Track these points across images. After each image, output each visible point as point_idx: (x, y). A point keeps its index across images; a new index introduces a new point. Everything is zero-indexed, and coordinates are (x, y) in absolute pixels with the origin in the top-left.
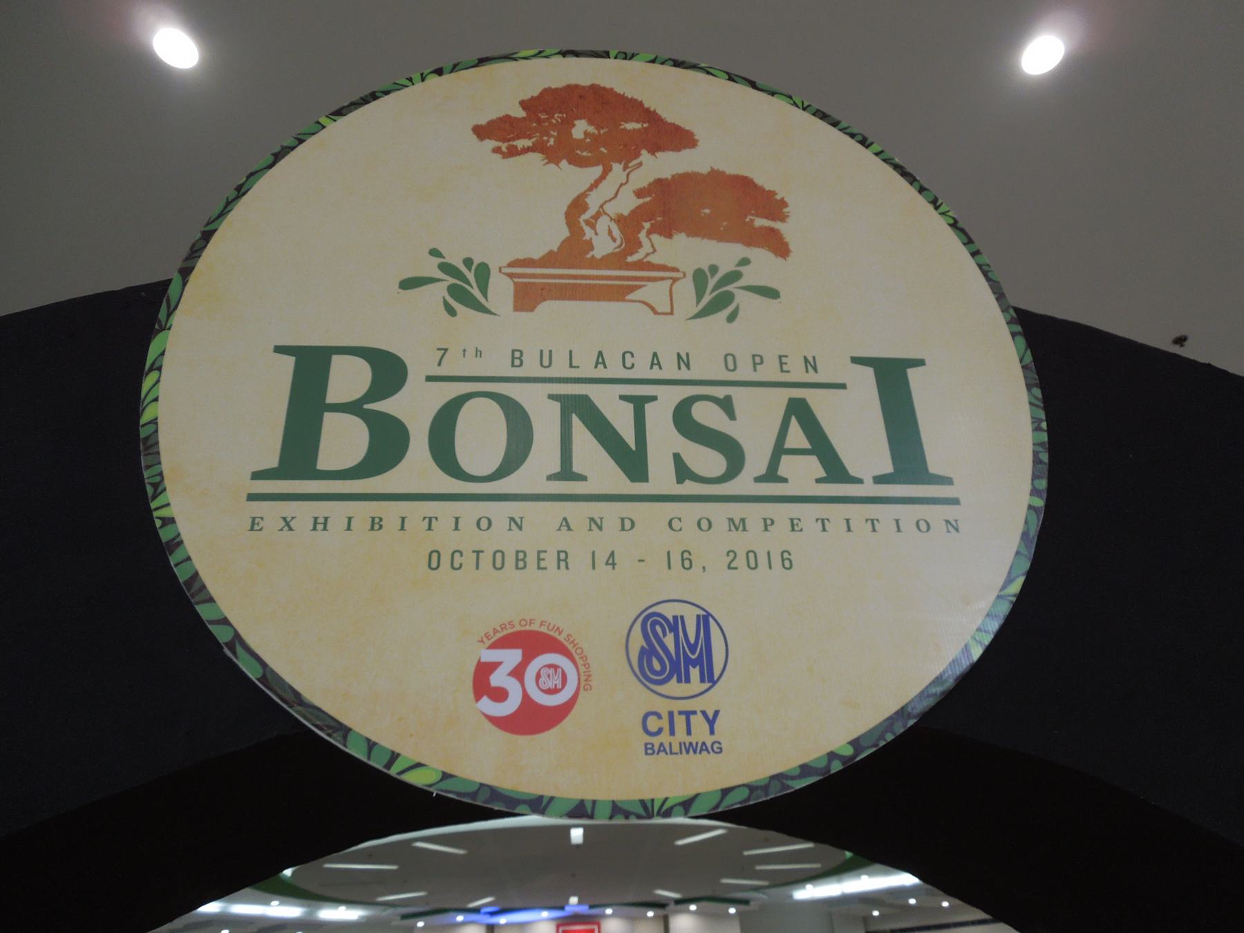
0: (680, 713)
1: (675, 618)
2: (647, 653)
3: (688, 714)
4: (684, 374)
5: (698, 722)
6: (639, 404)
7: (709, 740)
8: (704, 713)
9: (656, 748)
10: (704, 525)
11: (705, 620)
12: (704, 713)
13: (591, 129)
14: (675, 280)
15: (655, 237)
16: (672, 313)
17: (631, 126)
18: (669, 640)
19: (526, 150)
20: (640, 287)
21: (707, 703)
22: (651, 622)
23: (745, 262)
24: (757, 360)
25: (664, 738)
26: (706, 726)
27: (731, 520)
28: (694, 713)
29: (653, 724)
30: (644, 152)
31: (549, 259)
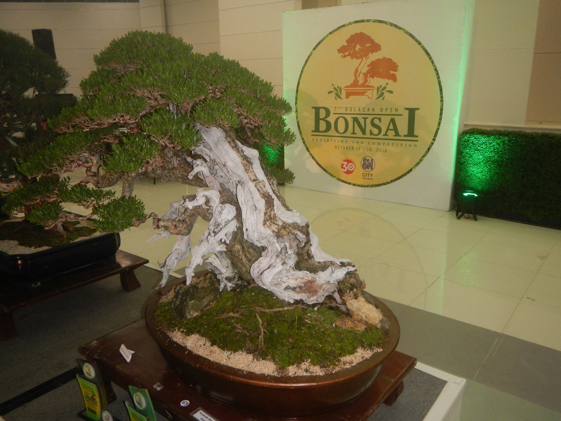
2: (364, 164)
3: (369, 174)
4: (373, 113)
5: (370, 175)
6: (365, 119)
7: (371, 178)
10: (374, 143)
11: (372, 160)
13: (360, 47)
14: (373, 90)
15: (370, 78)
16: (372, 98)
17: (368, 45)
18: (367, 163)
19: (348, 55)
20: (367, 92)
22: (364, 159)
23: (387, 84)
24: (386, 109)
25: (365, 177)
27: (378, 143)
29: (364, 175)
30: (370, 53)
31: (351, 86)
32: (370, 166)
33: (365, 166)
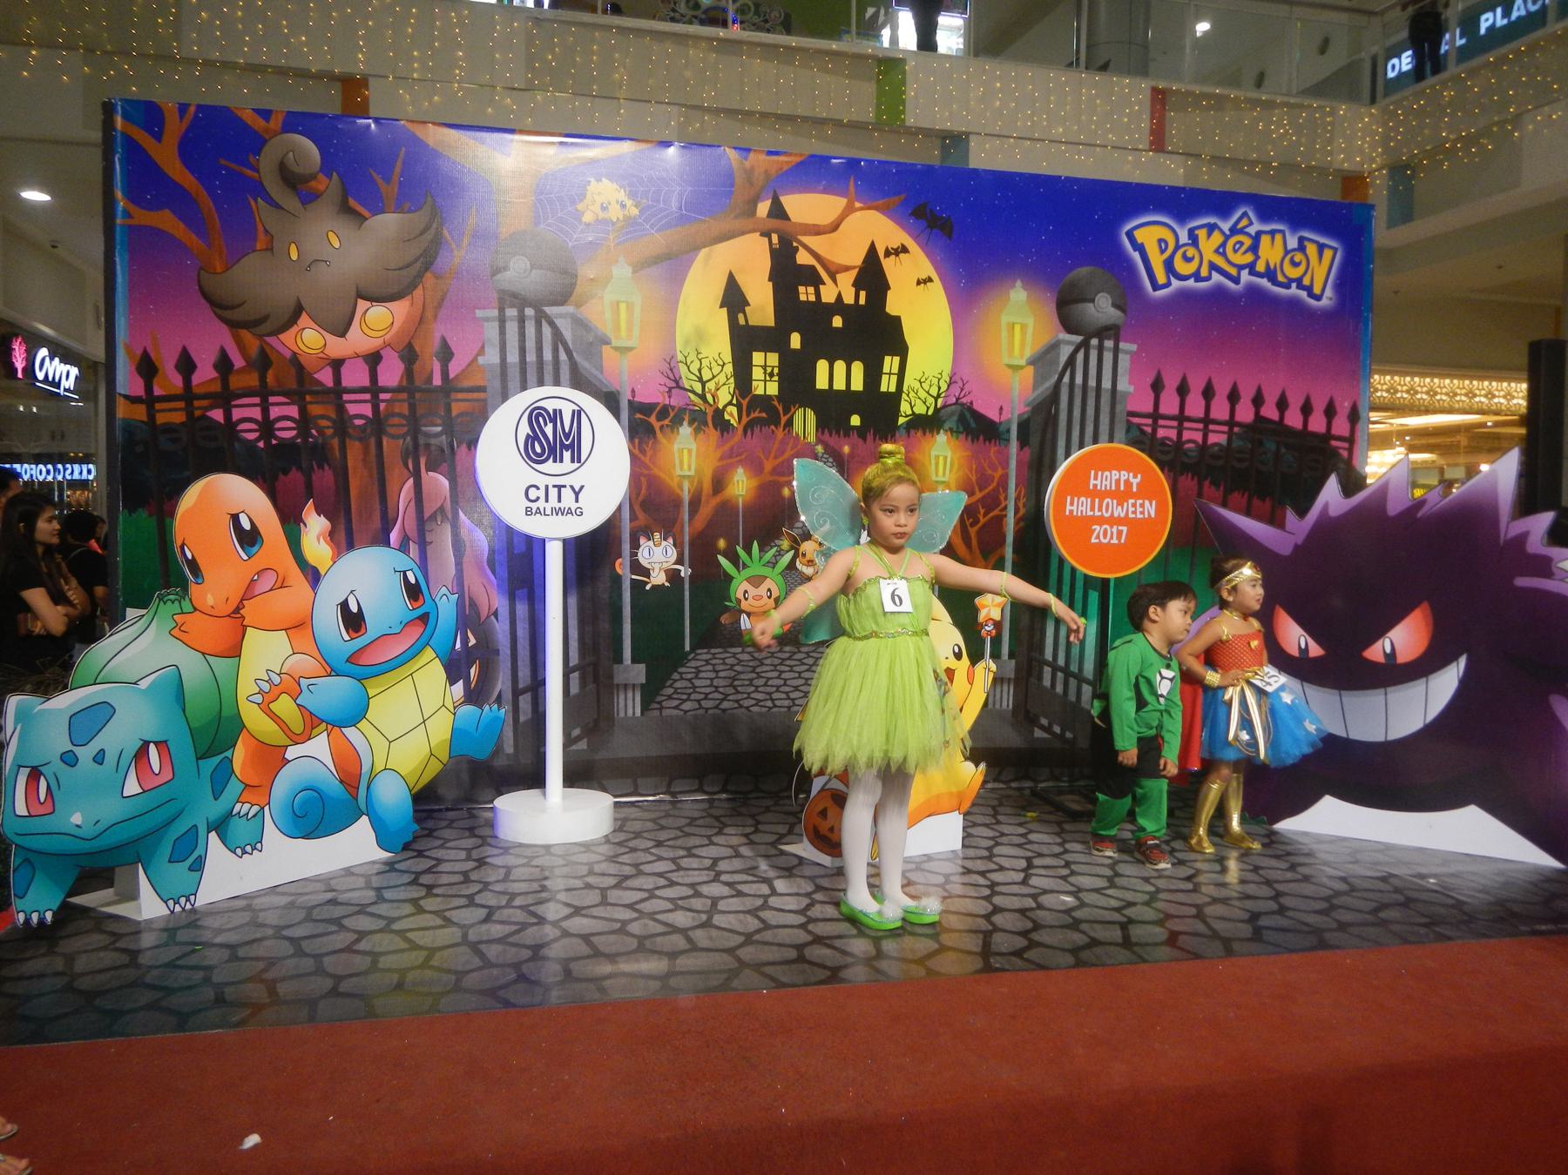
0: (554, 486)
1: (555, 411)
2: (531, 439)
3: (559, 487)
5: (567, 494)
7: (574, 506)
8: (572, 487)
9: (534, 511)
11: (577, 414)
12: (572, 487)
18: (549, 430)
21: (575, 480)
25: (541, 504)
26: (574, 496)
28: (565, 486)
29: (533, 494)
32: (567, 448)
33: (538, 449)
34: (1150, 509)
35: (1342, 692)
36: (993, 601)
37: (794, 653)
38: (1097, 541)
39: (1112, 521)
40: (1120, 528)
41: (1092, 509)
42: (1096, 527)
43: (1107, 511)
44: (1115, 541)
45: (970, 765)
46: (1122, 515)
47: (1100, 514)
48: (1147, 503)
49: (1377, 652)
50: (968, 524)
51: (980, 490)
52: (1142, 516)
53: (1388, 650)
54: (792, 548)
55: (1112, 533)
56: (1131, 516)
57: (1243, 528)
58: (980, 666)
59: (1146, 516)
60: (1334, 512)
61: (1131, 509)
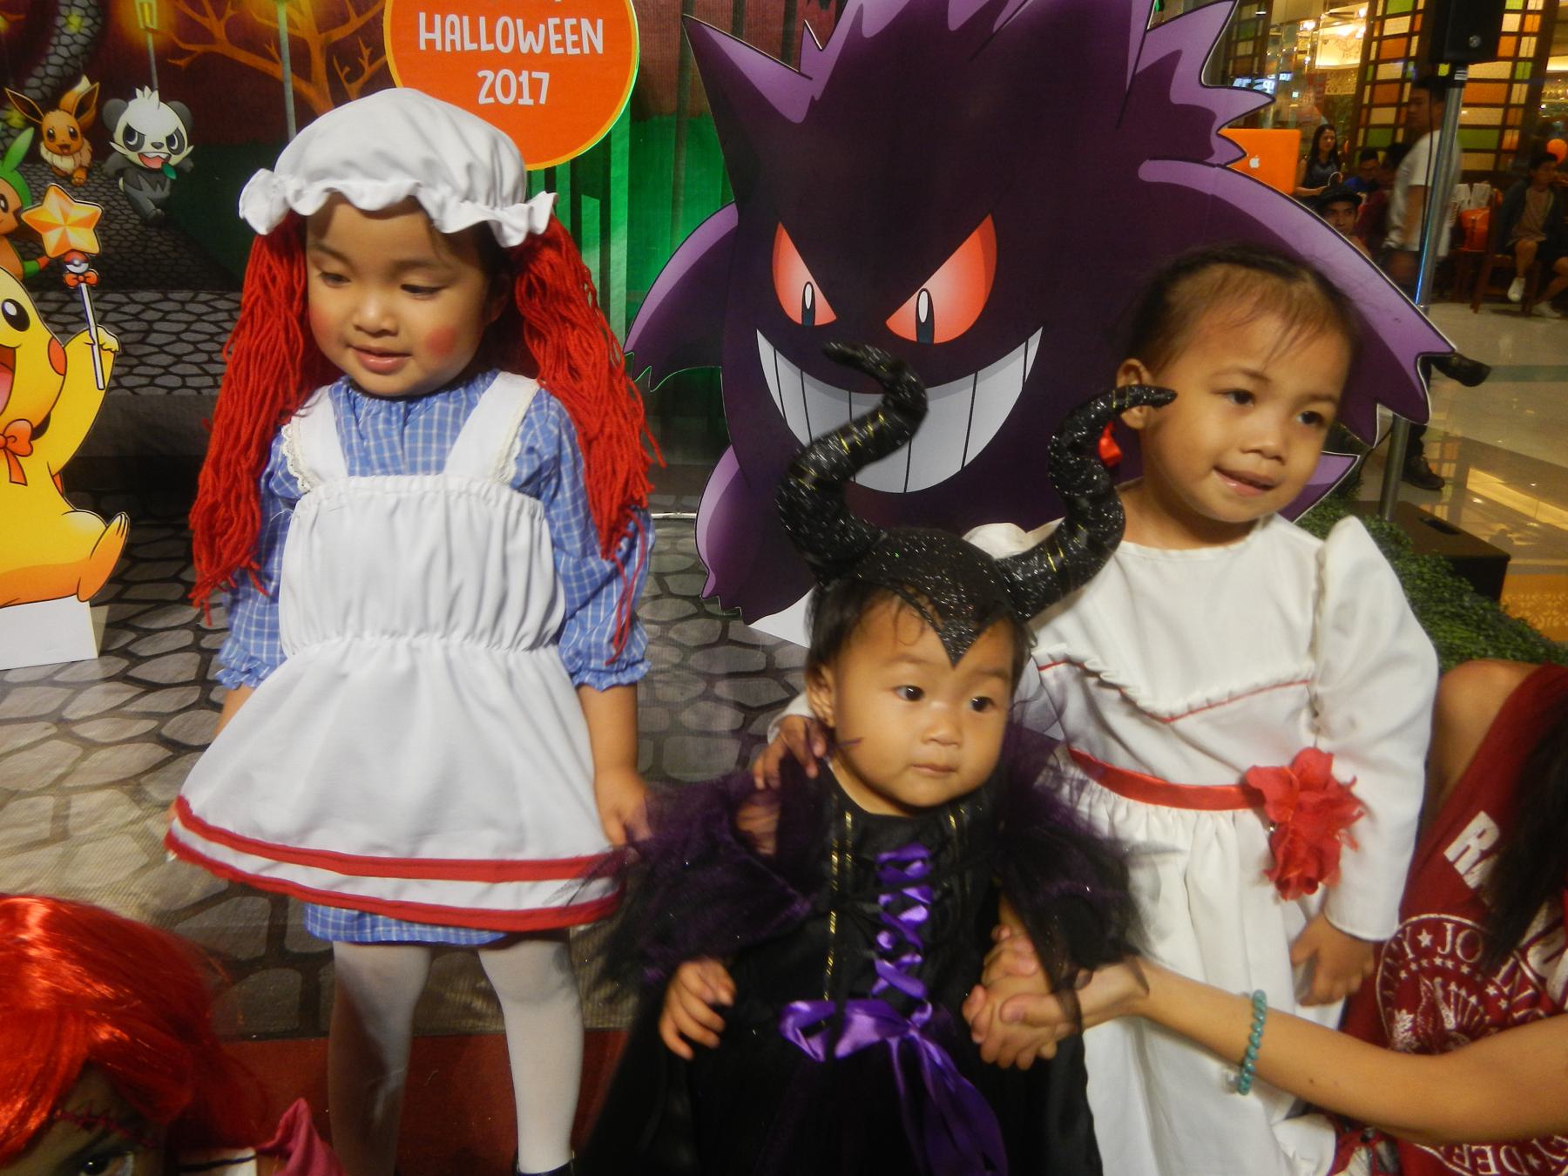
34: (593, 36)
35: (853, 394)
36: (65, 216)
37: (66, 303)
38: (491, 100)
39: (518, 61)
40: (536, 75)
41: (475, 37)
42: (489, 74)
43: (505, 42)
44: (526, 101)
45: (89, 522)
46: (538, 49)
47: (491, 47)
48: (585, 24)
49: (903, 322)
50: (342, 76)
51: (359, 13)
52: (577, 51)
53: (923, 318)
54: (28, 124)
55: (520, 85)
56: (555, 50)
57: (742, 68)
58: (78, 347)
59: (586, 50)
60: (870, 29)
61: (554, 38)
